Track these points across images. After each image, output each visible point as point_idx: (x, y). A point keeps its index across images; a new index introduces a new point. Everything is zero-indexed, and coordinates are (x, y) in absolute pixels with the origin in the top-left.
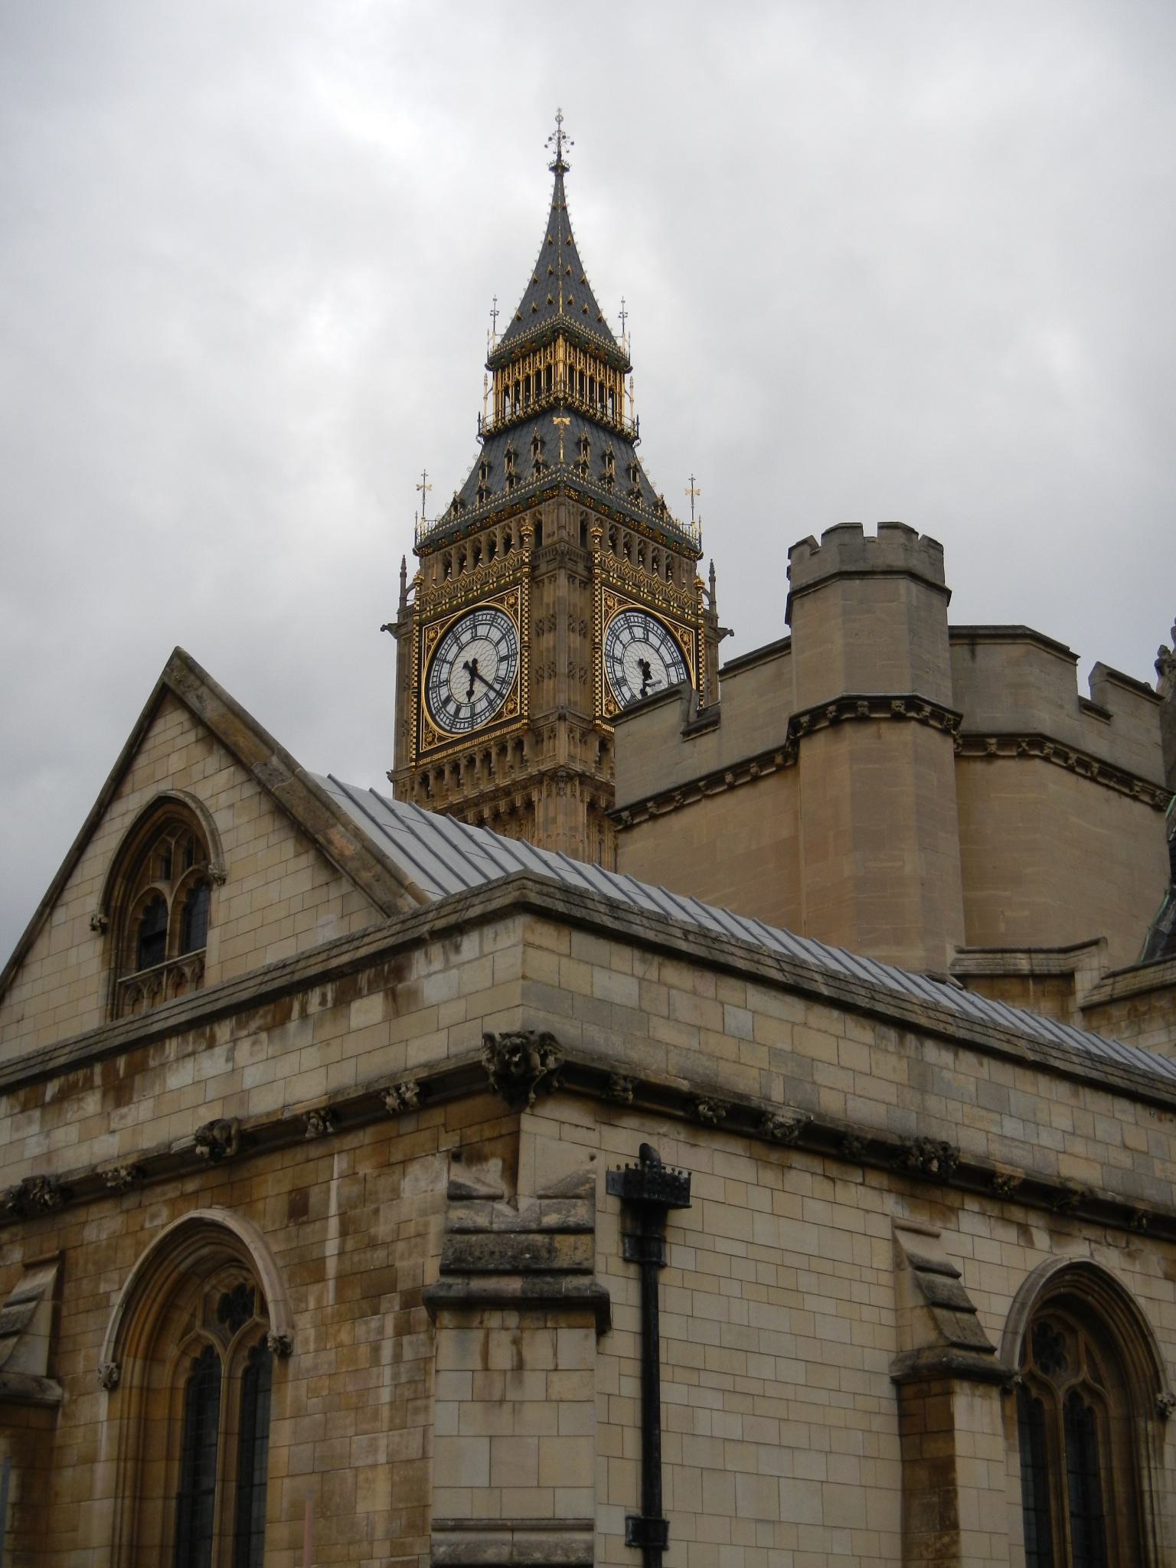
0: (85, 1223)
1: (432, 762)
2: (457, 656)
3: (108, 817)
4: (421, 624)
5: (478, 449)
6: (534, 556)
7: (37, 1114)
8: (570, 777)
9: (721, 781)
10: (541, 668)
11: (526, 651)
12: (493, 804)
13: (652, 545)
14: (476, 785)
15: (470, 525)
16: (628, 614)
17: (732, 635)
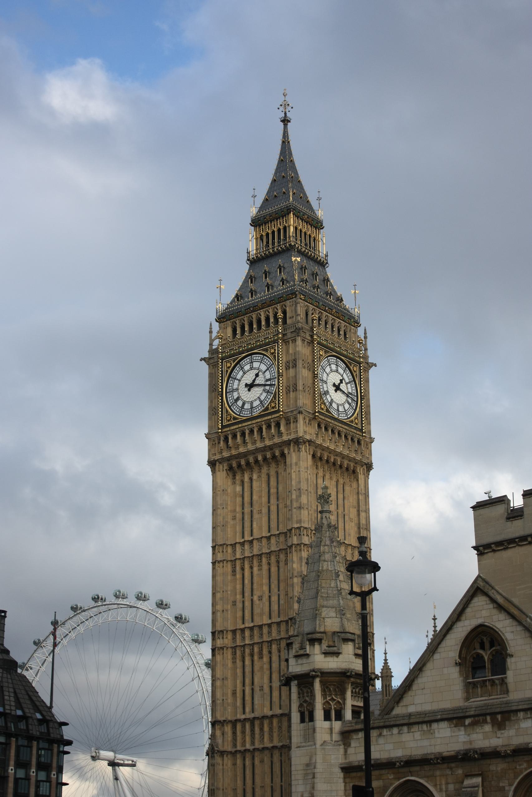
0: (490, 764)
1: (229, 430)
2: (242, 377)
3: (455, 626)
4: (222, 359)
5: (248, 267)
6: (284, 329)
7: (462, 728)
9: (526, 540)
10: (288, 386)
11: (281, 377)
12: (263, 453)
14: (254, 442)
15: (247, 309)
16: (329, 358)
17: (376, 366)
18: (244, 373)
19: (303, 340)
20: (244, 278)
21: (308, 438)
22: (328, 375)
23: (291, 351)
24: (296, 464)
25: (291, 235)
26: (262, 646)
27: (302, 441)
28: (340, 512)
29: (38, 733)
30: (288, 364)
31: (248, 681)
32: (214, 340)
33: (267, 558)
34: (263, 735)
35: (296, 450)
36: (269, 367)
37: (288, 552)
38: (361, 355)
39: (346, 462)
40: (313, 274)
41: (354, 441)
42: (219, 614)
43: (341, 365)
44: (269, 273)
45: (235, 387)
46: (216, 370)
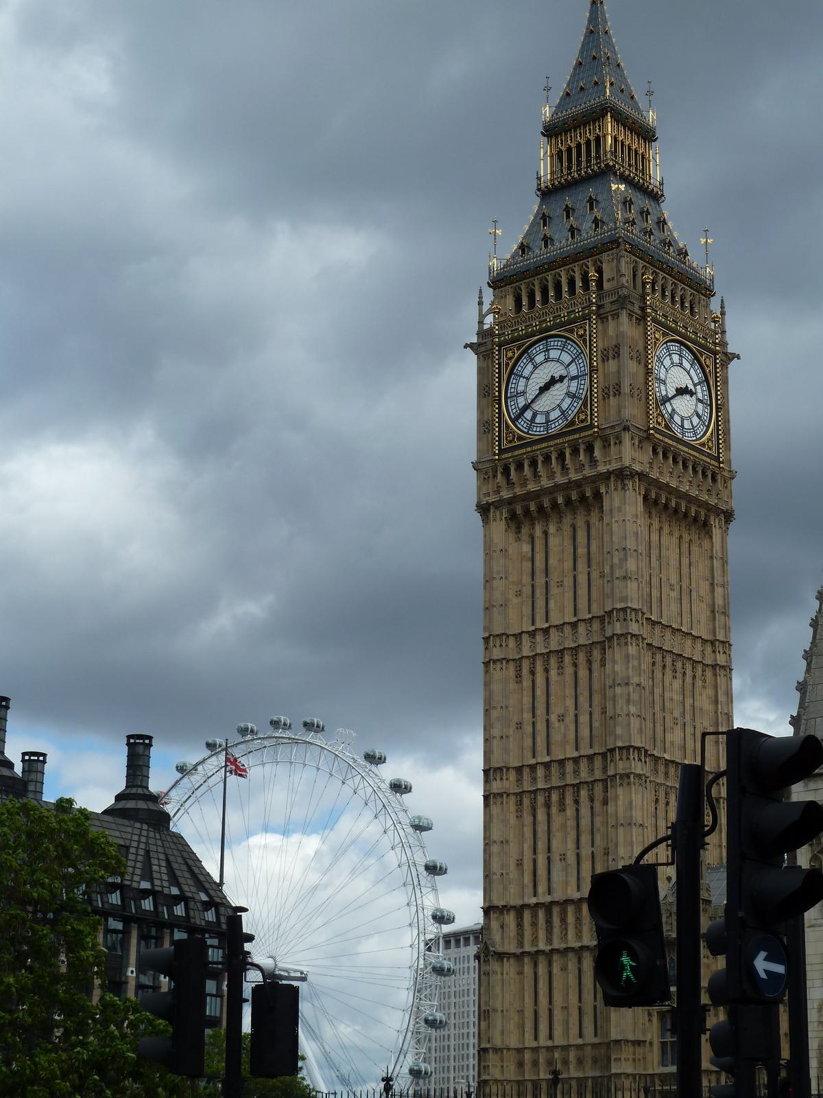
1: (512, 457)
2: (532, 373)
4: (500, 345)
6: (599, 297)
8: (634, 475)
13: (681, 286)
14: (552, 475)
16: (668, 344)
19: (630, 315)
24: (619, 509)
25: (608, 149)
26: (563, 791)
27: (628, 473)
28: (684, 587)
29: (203, 923)
30: (605, 352)
31: (541, 845)
34: (566, 929)
35: (620, 487)
37: (607, 646)
38: (717, 341)
40: (642, 213)
42: (495, 742)
43: (687, 355)
44: (573, 210)
45: (521, 389)
46: (490, 363)
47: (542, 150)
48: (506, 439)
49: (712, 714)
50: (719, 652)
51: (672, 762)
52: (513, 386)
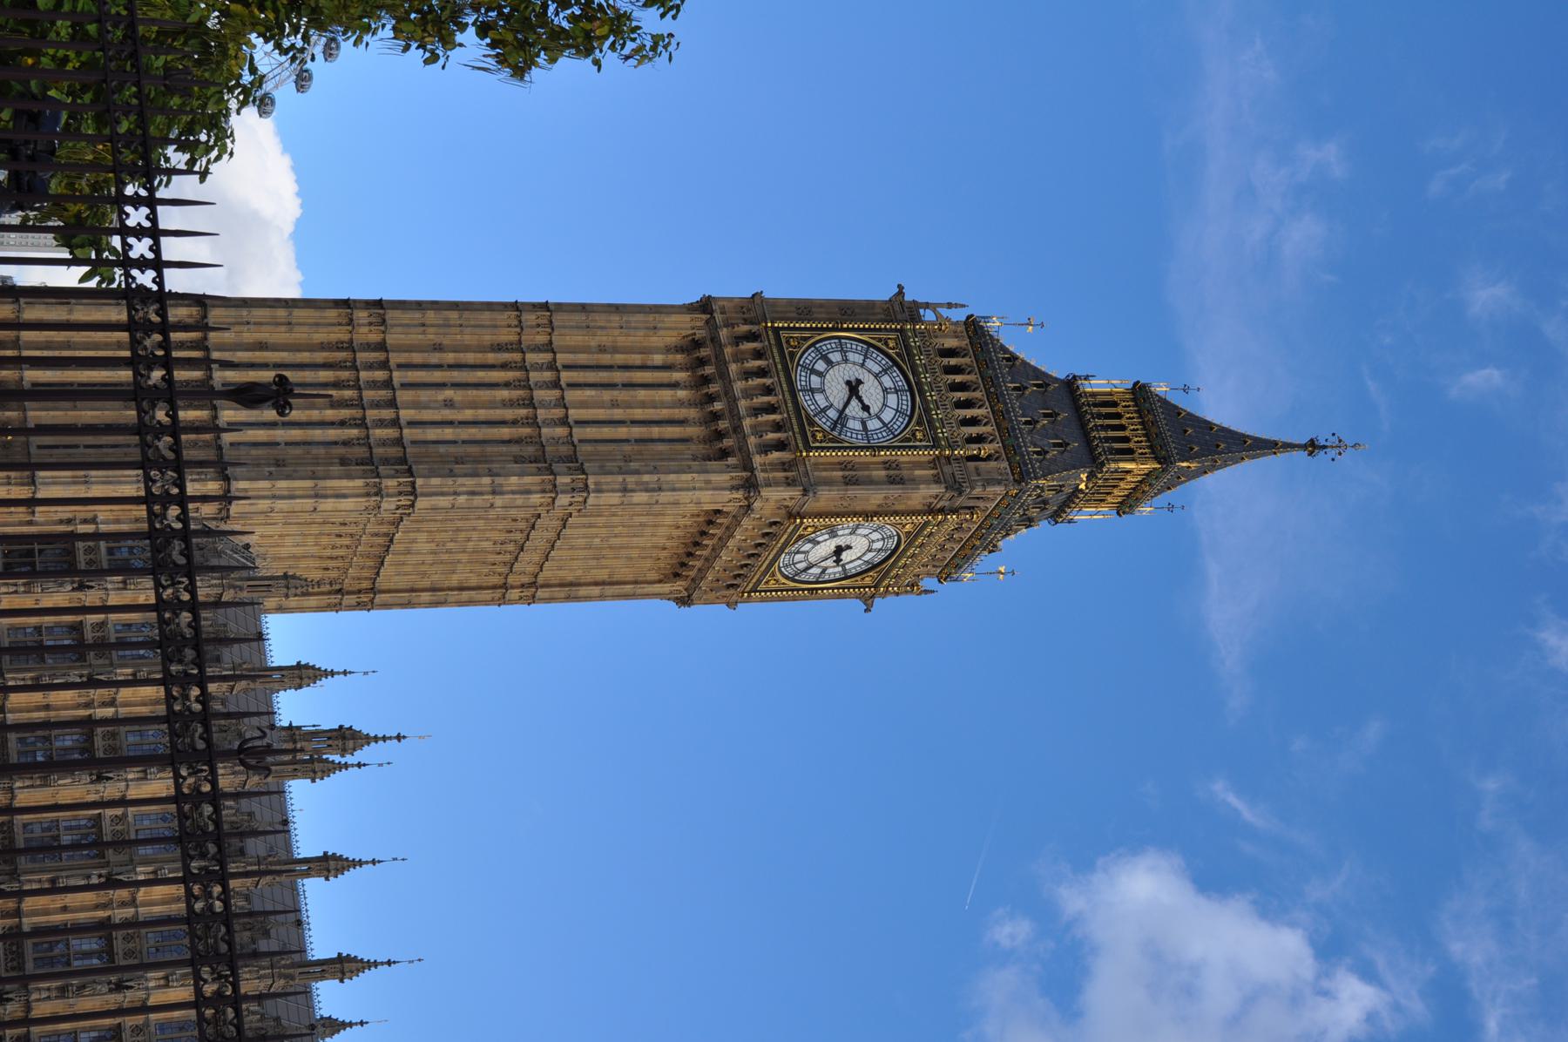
2: (870, 371)
4: (902, 331)
10: (853, 466)
11: (871, 454)
12: (727, 413)
14: (748, 394)
15: (992, 381)
16: (896, 538)
18: (878, 374)
20: (1043, 369)
21: (755, 504)
22: (865, 536)
23: (917, 472)
27: (752, 494)
32: (934, 310)
33: (527, 419)
35: (735, 483)
36: (888, 428)
37: (540, 465)
38: (890, 589)
39: (698, 564)
41: (735, 578)
42: (417, 315)
45: (851, 356)
46: (879, 317)
47: (1119, 382)
48: (791, 337)
49: (447, 584)
50: (522, 592)
51: (391, 541)
52: (854, 347)
